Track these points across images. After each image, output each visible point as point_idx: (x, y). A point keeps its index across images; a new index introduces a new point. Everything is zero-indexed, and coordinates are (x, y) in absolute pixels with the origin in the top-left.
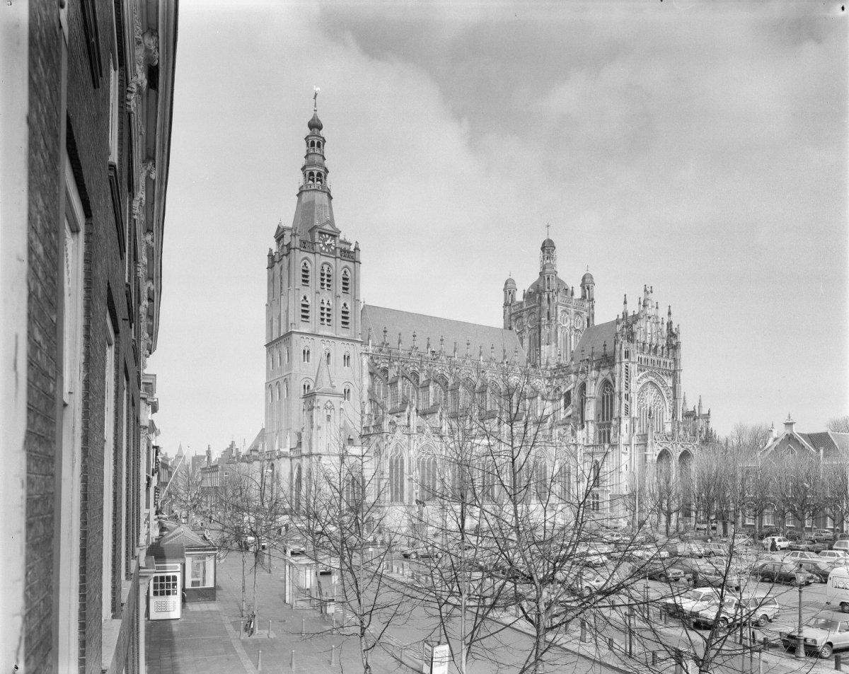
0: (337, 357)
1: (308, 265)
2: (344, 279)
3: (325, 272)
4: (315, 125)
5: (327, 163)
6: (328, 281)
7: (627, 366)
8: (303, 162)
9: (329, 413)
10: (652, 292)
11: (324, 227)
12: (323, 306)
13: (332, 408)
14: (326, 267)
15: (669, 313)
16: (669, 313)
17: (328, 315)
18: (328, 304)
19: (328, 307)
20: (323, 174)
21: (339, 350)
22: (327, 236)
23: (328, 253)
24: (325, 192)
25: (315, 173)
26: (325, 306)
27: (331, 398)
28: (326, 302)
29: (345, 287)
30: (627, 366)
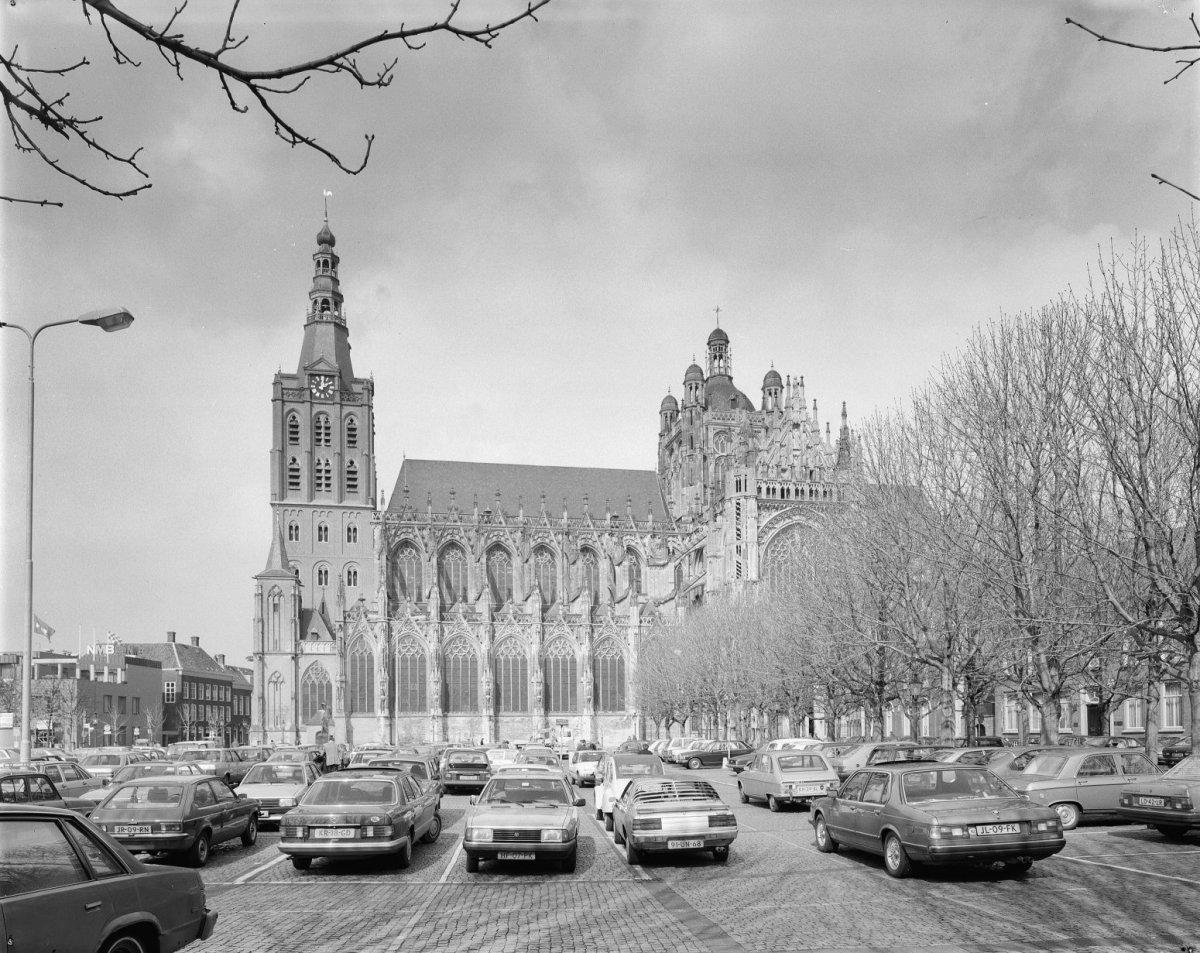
0: (337, 530)
1: (298, 418)
2: (349, 429)
3: (323, 424)
4: (327, 240)
5: (342, 289)
6: (327, 434)
7: (738, 504)
8: (310, 286)
9: (276, 601)
10: (802, 385)
11: (317, 367)
12: (319, 467)
13: (280, 595)
14: (322, 418)
15: (844, 415)
16: (844, 415)
17: (328, 478)
18: (327, 464)
19: (327, 468)
20: (330, 300)
21: (336, 523)
22: (323, 378)
23: (326, 398)
24: (330, 322)
25: (320, 300)
26: (322, 467)
27: (276, 582)
28: (323, 462)
29: (352, 439)
30: (738, 504)
